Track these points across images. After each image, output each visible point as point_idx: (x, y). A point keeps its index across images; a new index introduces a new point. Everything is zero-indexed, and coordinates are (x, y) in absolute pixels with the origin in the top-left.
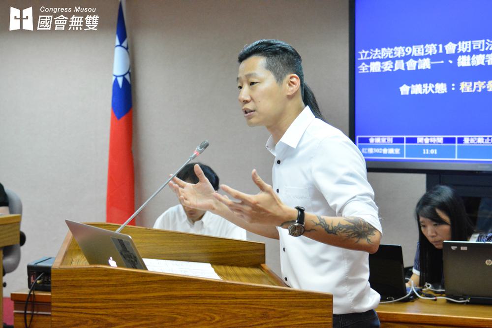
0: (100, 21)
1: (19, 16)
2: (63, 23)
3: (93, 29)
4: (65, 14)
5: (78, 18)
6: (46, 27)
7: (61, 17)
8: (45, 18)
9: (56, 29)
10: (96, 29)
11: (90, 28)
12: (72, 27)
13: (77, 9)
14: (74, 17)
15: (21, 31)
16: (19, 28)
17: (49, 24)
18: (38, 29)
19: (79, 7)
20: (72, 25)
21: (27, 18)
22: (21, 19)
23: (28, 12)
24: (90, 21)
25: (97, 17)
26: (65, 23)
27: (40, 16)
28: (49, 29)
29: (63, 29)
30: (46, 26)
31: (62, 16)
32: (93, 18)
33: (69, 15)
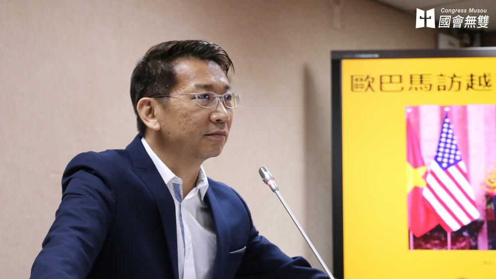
0: (489, 20)
1: (423, 17)
2: (460, 22)
3: (484, 27)
4: (461, 14)
5: (472, 17)
6: (446, 26)
7: (458, 17)
8: (445, 18)
9: (454, 27)
10: (487, 27)
11: (482, 26)
12: (467, 25)
13: (471, 10)
14: (468, 17)
15: (425, 29)
16: (423, 26)
17: (448, 23)
18: (439, 27)
19: (473, 9)
20: (467, 24)
21: (430, 18)
22: (425, 19)
23: (431, 13)
24: (481, 21)
25: (488, 17)
26: (462, 22)
27: (441, 16)
28: (449, 27)
29: (460, 27)
30: (446, 24)
31: (459, 16)
32: (484, 18)
33: (464, 15)
